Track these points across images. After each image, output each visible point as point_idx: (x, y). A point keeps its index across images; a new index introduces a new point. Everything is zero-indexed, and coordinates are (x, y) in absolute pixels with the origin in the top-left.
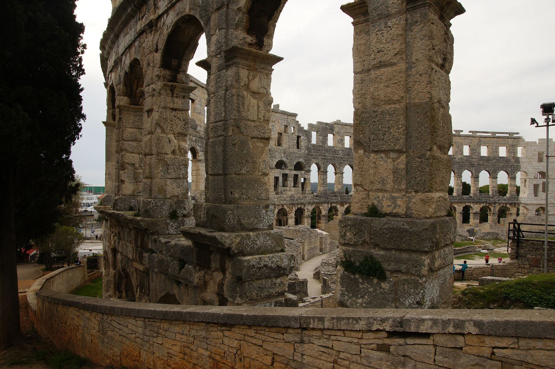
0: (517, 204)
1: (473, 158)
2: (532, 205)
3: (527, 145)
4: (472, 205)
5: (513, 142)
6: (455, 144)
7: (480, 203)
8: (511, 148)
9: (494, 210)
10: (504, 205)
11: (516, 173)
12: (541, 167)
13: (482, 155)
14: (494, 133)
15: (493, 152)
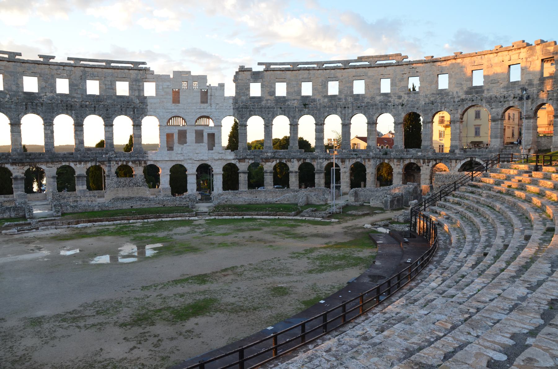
0: (143, 162)
1: (74, 97)
2: (164, 162)
3: (159, 79)
4: (72, 165)
5: (137, 75)
6: (40, 76)
7: (86, 162)
8: (134, 83)
9: (109, 171)
10: (125, 163)
11: (142, 119)
12: (176, 111)
13: (88, 93)
14: (109, 62)
15: (106, 89)
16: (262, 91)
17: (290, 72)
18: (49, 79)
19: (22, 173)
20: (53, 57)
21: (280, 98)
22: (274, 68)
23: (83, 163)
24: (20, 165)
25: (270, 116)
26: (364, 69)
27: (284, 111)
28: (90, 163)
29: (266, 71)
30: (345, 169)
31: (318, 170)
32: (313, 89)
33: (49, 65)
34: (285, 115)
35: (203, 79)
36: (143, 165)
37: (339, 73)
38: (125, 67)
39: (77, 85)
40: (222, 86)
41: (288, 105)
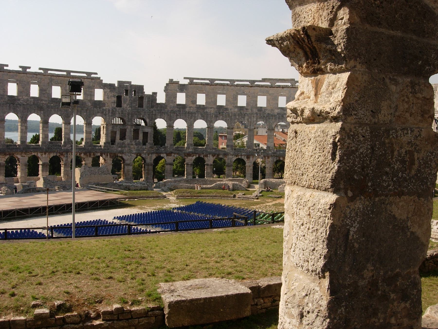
0: (92, 154)
1: (42, 100)
4: (39, 155)
7: (50, 152)
8: (88, 90)
11: (92, 119)
13: (53, 97)
16: (186, 100)
17: (209, 86)
18: (26, 85)
19: (4, 161)
20: (29, 68)
21: (200, 105)
22: (197, 82)
23: (47, 153)
24: (3, 154)
25: (192, 120)
26: (266, 88)
27: (204, 117)
28: (52, 153)
29: (190, 84)
30: (249, 164)
31: (228, 164)
32: (226, 101)
33: (26, 74)
34: (204, 120)
35: (141, 88)
36: (92, 156)
37: (247, 90)
38: (82, 76)
39: (45, 90)
40: (155, 94)
41: (207, 112)
